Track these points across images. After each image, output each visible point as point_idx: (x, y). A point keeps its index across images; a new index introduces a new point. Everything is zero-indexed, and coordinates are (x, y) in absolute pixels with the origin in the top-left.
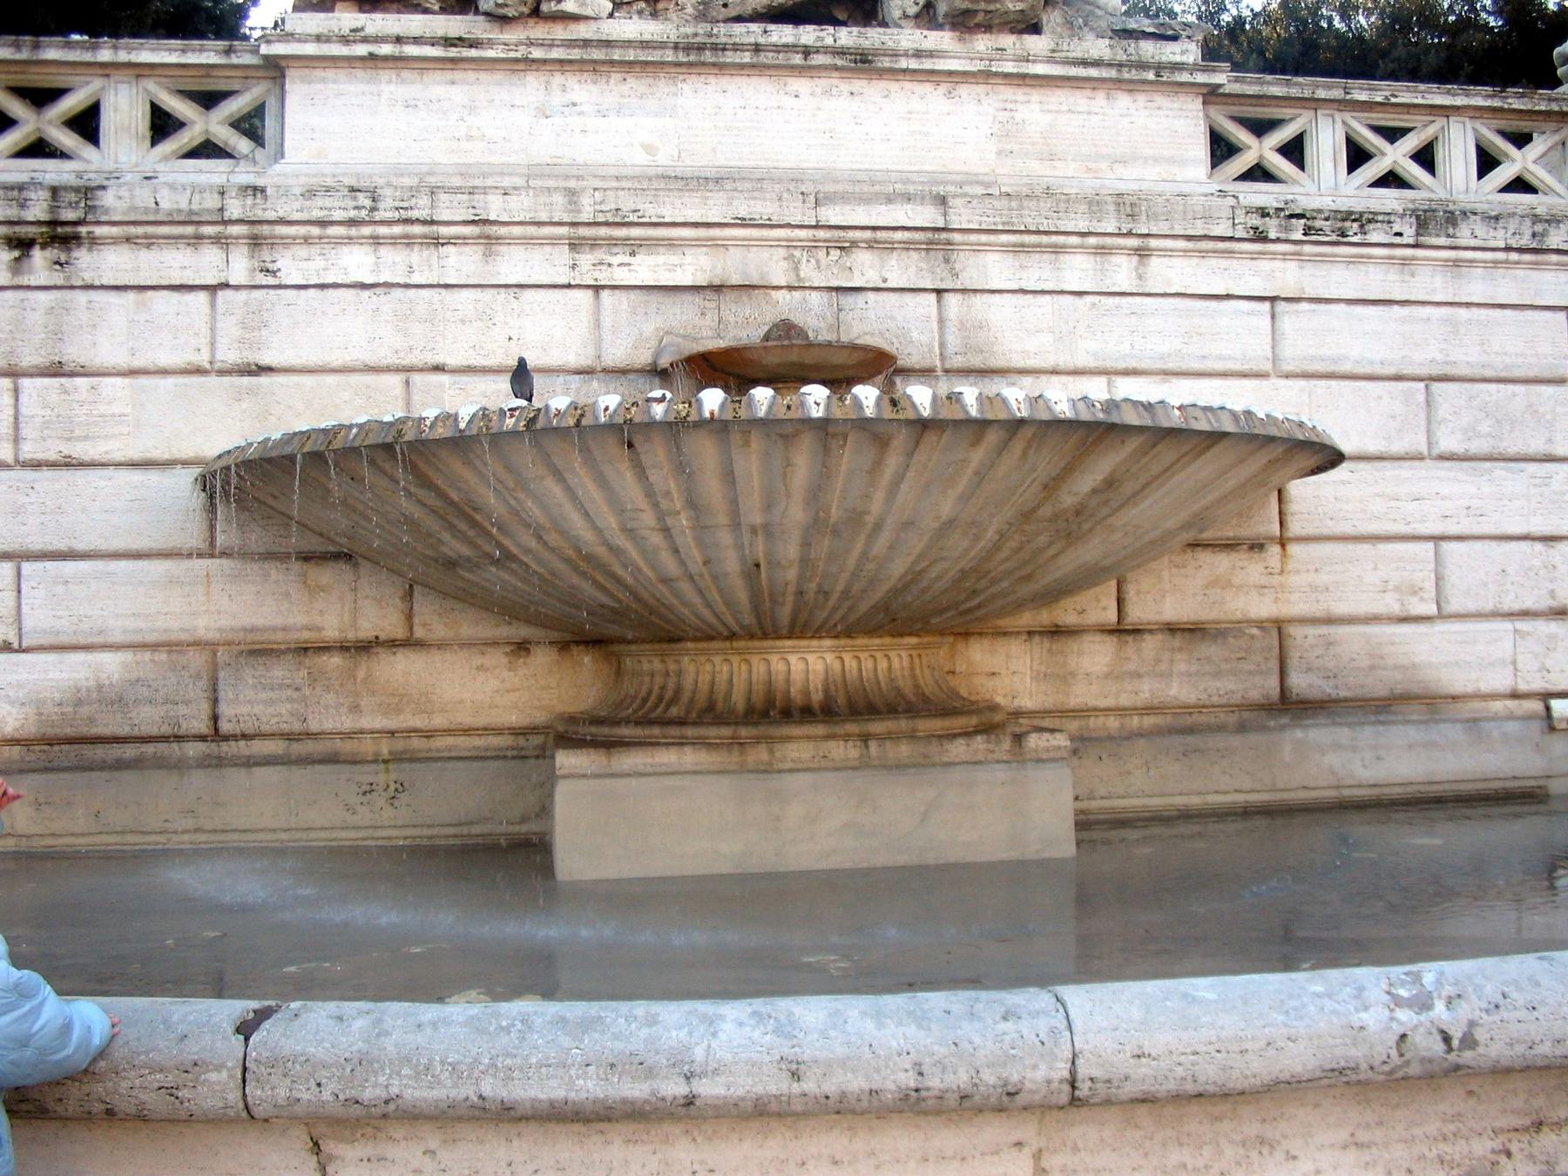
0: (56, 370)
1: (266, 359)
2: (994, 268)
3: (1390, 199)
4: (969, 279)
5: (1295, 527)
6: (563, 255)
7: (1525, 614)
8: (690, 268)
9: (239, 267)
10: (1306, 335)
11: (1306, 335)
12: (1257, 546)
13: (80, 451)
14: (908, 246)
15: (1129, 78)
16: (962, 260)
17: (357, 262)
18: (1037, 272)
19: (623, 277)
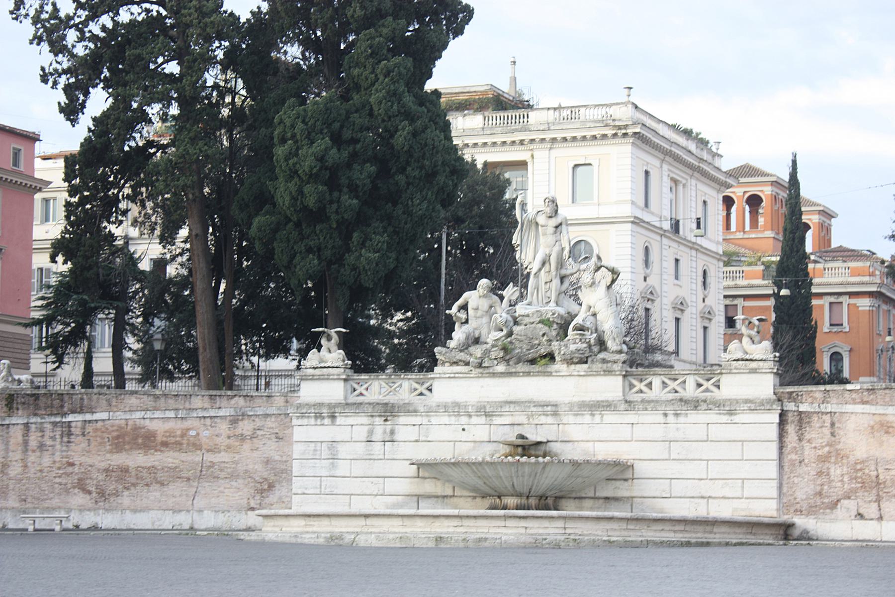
0: (393, 441)
1: (429, 439)
2: (570, 419)
3: (671, 396)
4: (565, 421)
5: (635, 476)
6: (484, 418)
7: (693, 497)
8: (507, 420)
9: (425, 421)
10: (639, 432)
11: (639, 432)
12: (626, 480)
13: (395, 457)
14: (552, 415)
15: (609, 372)
16: (563, 417)
17: (445, 419)
18: (579, 419)
19: (495, 422)
